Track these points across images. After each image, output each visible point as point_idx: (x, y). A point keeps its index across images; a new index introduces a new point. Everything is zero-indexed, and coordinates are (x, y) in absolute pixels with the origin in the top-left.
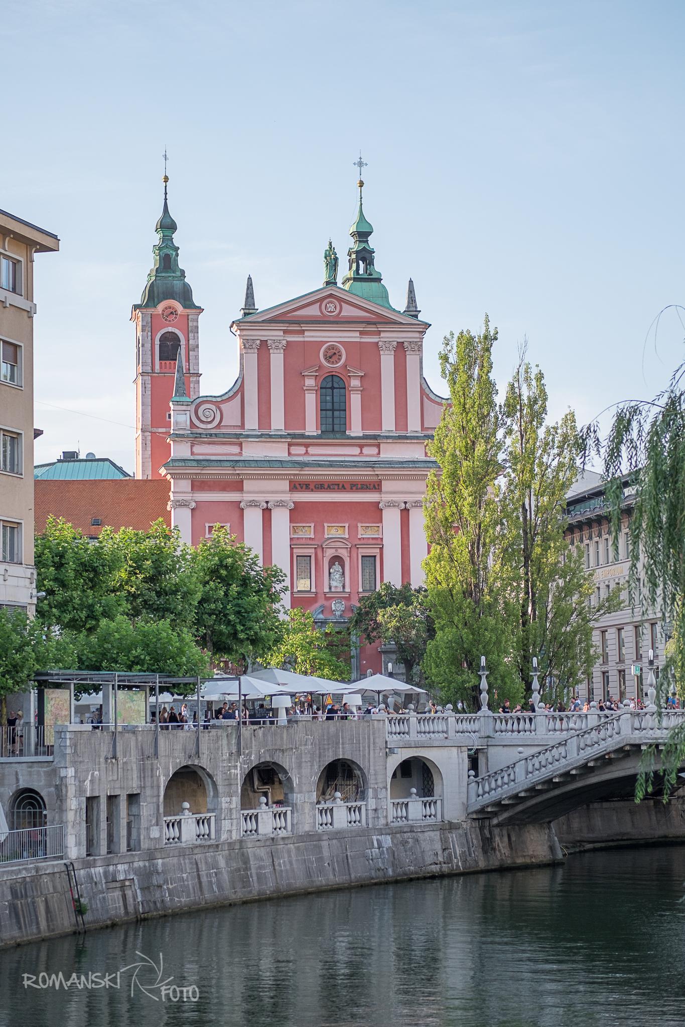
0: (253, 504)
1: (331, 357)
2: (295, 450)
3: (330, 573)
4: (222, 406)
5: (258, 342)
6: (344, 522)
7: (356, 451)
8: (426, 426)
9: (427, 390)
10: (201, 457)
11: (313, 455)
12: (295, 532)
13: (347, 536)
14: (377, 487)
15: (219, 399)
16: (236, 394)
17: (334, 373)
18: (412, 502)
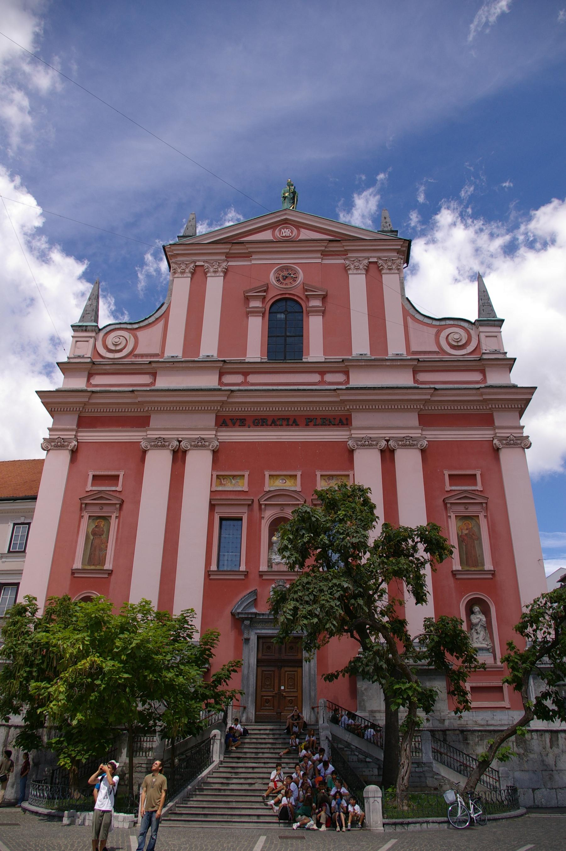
0: (160, 444)
1: (285, 278)
2: (228, 379)
3: (271, 544)
4: (139, 334)
5: (192, 265)
6: (295, 469)
7: (316, 378)
8: (414, 348)
9: (412, 311)
10: (98, 389)
11: (253, 384)
12: (221, 484)
13: (298, 488)
14: (345, 423)
15: (136, 326)
16: (157, 319)
17: (287, 296)
18: (397, 439)
